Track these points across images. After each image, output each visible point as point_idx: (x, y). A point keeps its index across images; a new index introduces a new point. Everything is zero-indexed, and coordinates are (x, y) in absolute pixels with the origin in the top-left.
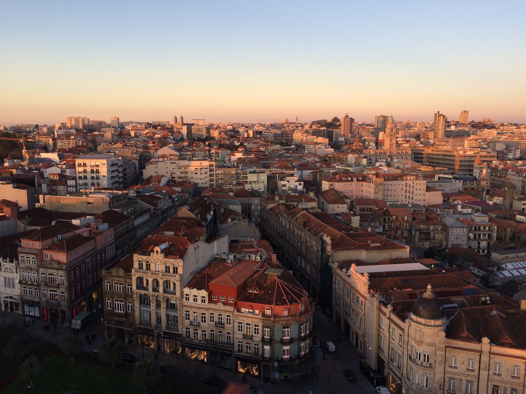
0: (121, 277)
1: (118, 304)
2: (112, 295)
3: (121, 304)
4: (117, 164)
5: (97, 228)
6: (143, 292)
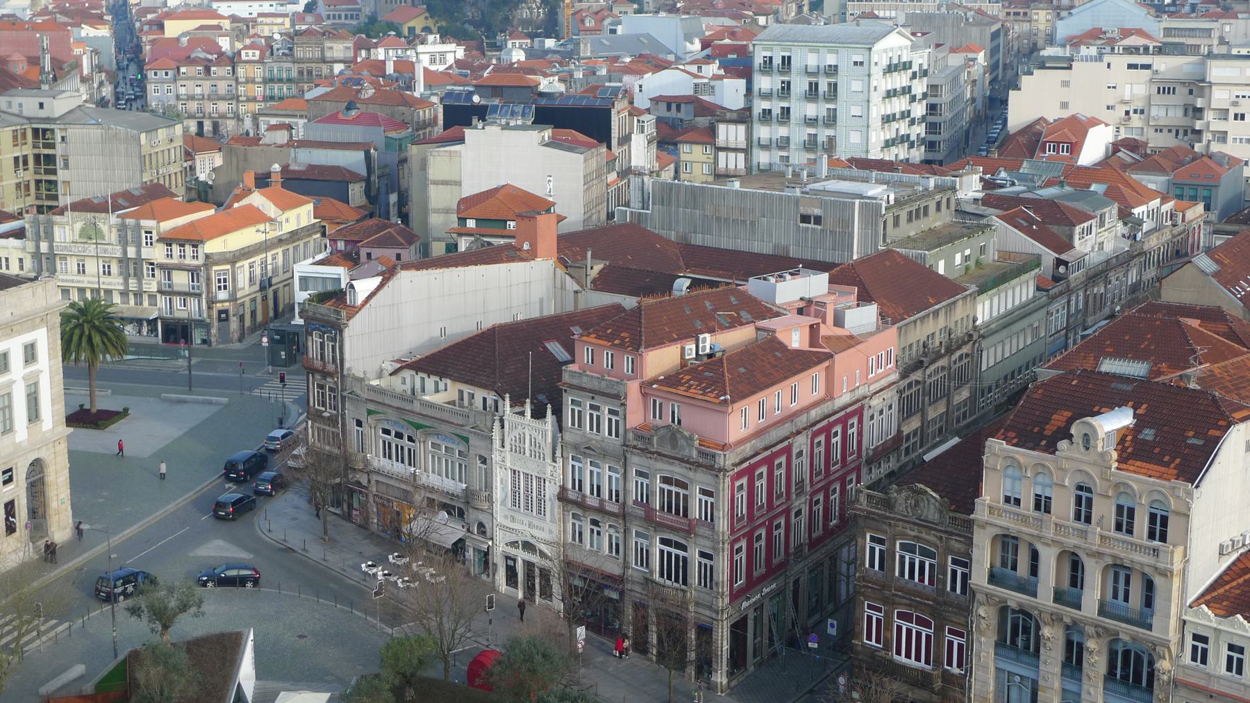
0: (925, 524)
1: (909, 631)
2: (886, 592)
3: (919, 634)
4: (907, 66)
5: (839, 321)
6: (1015, 598)
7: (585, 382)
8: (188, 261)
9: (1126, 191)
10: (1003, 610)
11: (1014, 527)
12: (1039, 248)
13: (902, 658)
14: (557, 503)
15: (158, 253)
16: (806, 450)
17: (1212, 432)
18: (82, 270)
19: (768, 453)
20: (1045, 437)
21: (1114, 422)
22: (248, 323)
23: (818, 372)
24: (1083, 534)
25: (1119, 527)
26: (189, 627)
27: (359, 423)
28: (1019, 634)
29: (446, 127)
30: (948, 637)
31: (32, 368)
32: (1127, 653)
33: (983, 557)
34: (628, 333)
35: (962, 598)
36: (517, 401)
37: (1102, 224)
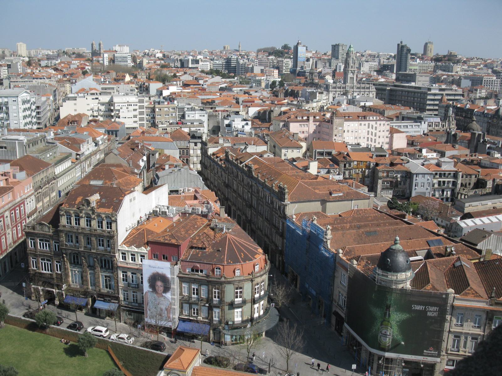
1: (45, 263)
3: (48, 264)
4: (29, 101)
5: (14, 177)
9: (94, 133)
13: (44, 272)
16: (9, 216)
17: (120, 198)
20: (76, 204)
32: (105, 260)
37: (88, 143)
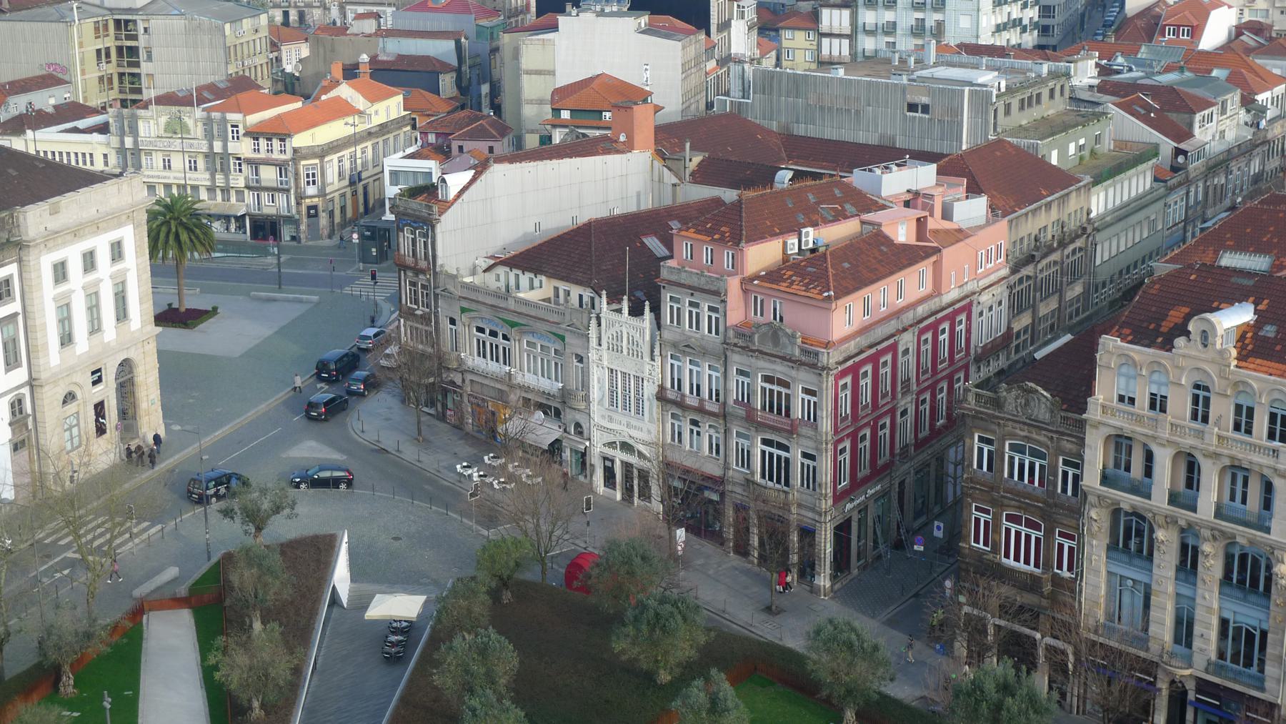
0: (1036, 425)
1: (1018, 534)
2: (994, 494)
3: (1028, 537)
5: (947, 214)
6: (1128, 500)
7: (684, 278)
8: (276, 155)
9: (1249, 77)
10: (1116, 512)
11: (1128, 427)
12: (1155, 136)
13: (1011, 562)
14: (655, 402)
15: (244, 148)
18: (167, 166)
19: (873, 351)
20: (1162, 334)
21: (1233, 319)
22: (337, 219)
23: (925, 267)
24: (1200, 435)
25: (1237, 427)
26: (282, 529)
27: (453, 322)
28: (1132, 537)
29: (539, 14)
30: (1059, 540)
31: (119, 266)
32: (1243, 557)
33: (1096, 457)
34: (729, 227)
35: (1074, 500)
36: (614, 298)
37: (1223, 111)
